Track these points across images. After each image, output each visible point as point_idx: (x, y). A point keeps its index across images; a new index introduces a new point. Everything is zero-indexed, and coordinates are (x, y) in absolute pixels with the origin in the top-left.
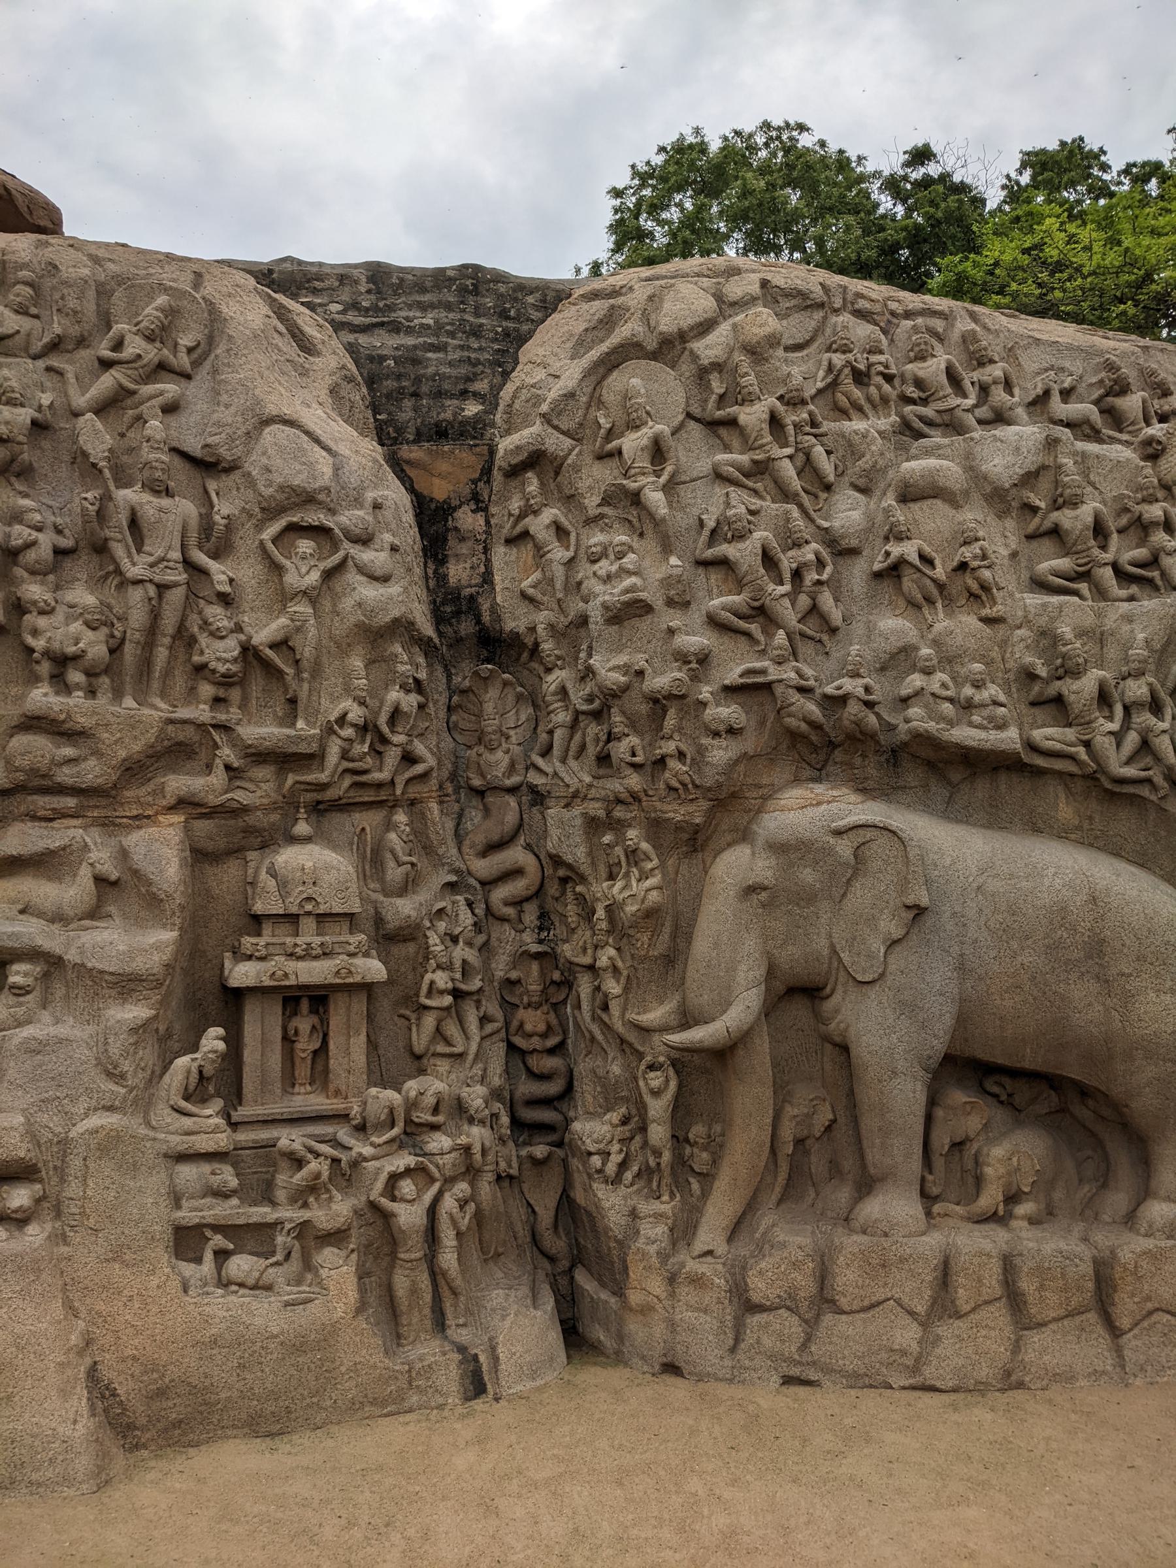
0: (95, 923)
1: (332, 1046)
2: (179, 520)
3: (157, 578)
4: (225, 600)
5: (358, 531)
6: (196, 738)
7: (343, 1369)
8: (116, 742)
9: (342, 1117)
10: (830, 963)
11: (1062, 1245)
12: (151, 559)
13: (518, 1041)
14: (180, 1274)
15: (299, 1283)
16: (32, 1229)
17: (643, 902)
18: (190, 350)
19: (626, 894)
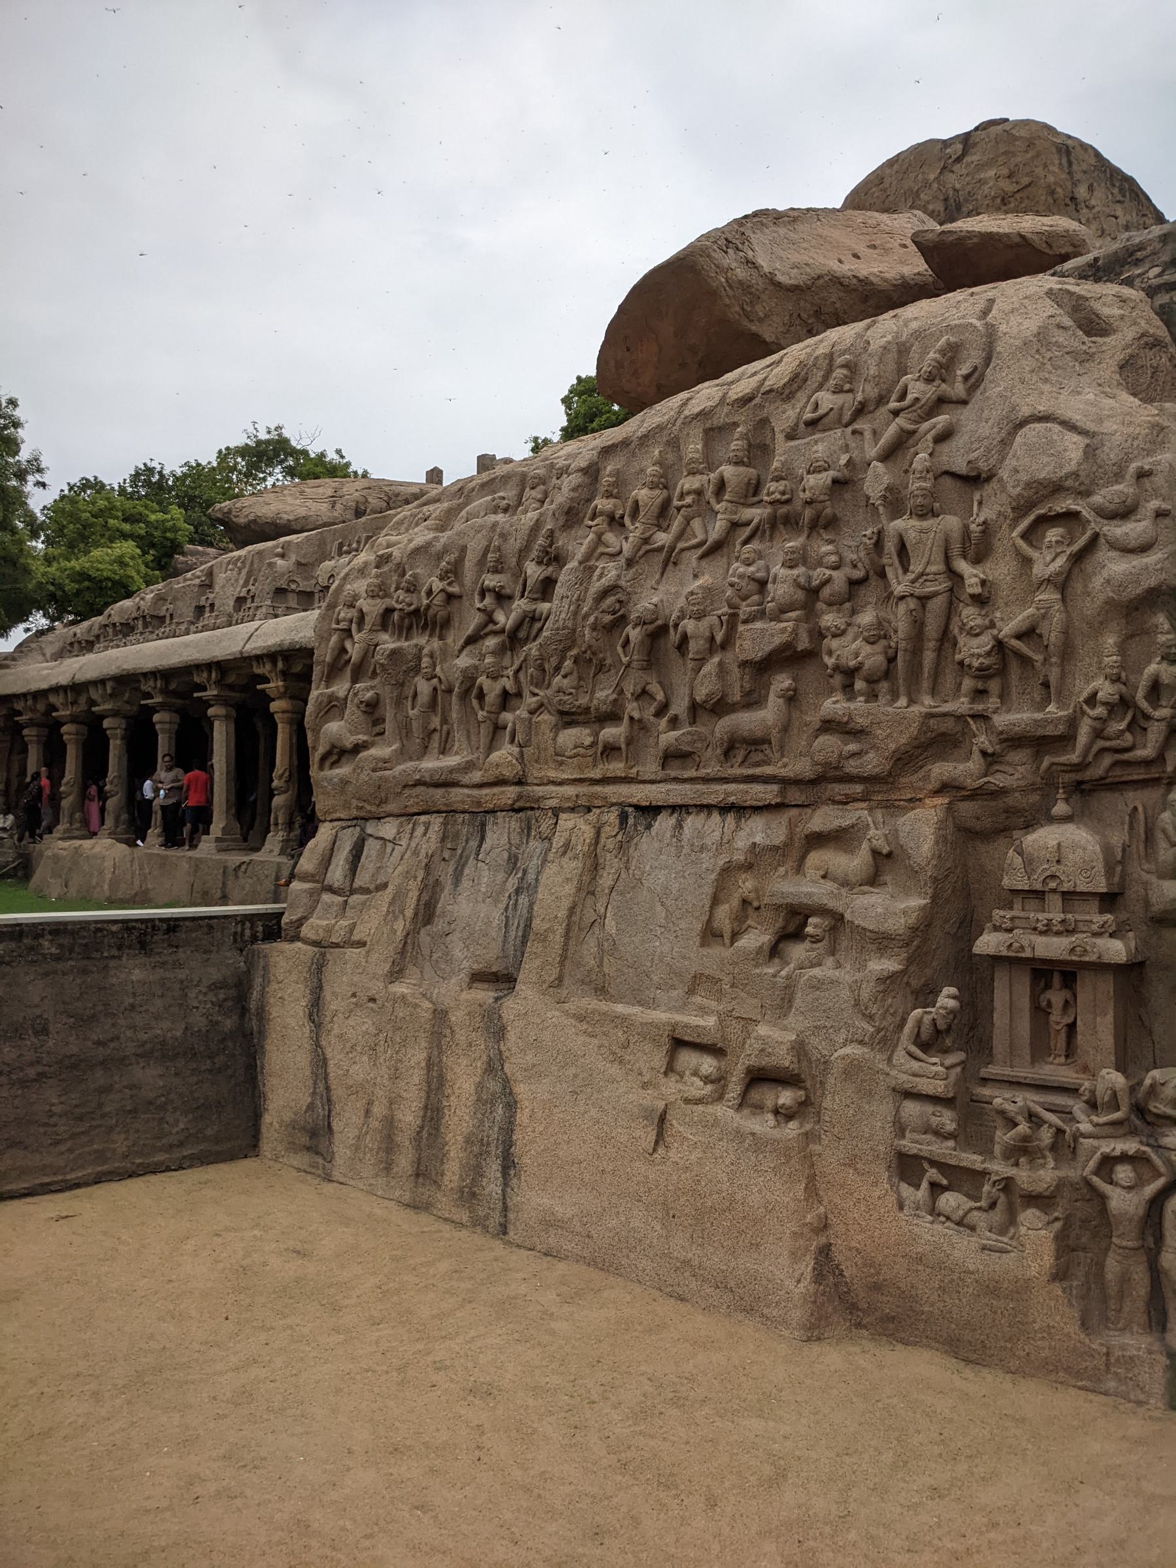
0: (872, 889)
1: (1079, 1023)
2: (940, 536)
3: (918, 592)
4: (980, 601)
5: (1112, 507)
6: (959, 728)
7: (1037, 1326)
8: (887, 736)
9: (1073, 1091)
12: (911, 576)
14: (899, 1193)
15: (1002, 1231)
16: (793, 1125)
18: (966, 378)
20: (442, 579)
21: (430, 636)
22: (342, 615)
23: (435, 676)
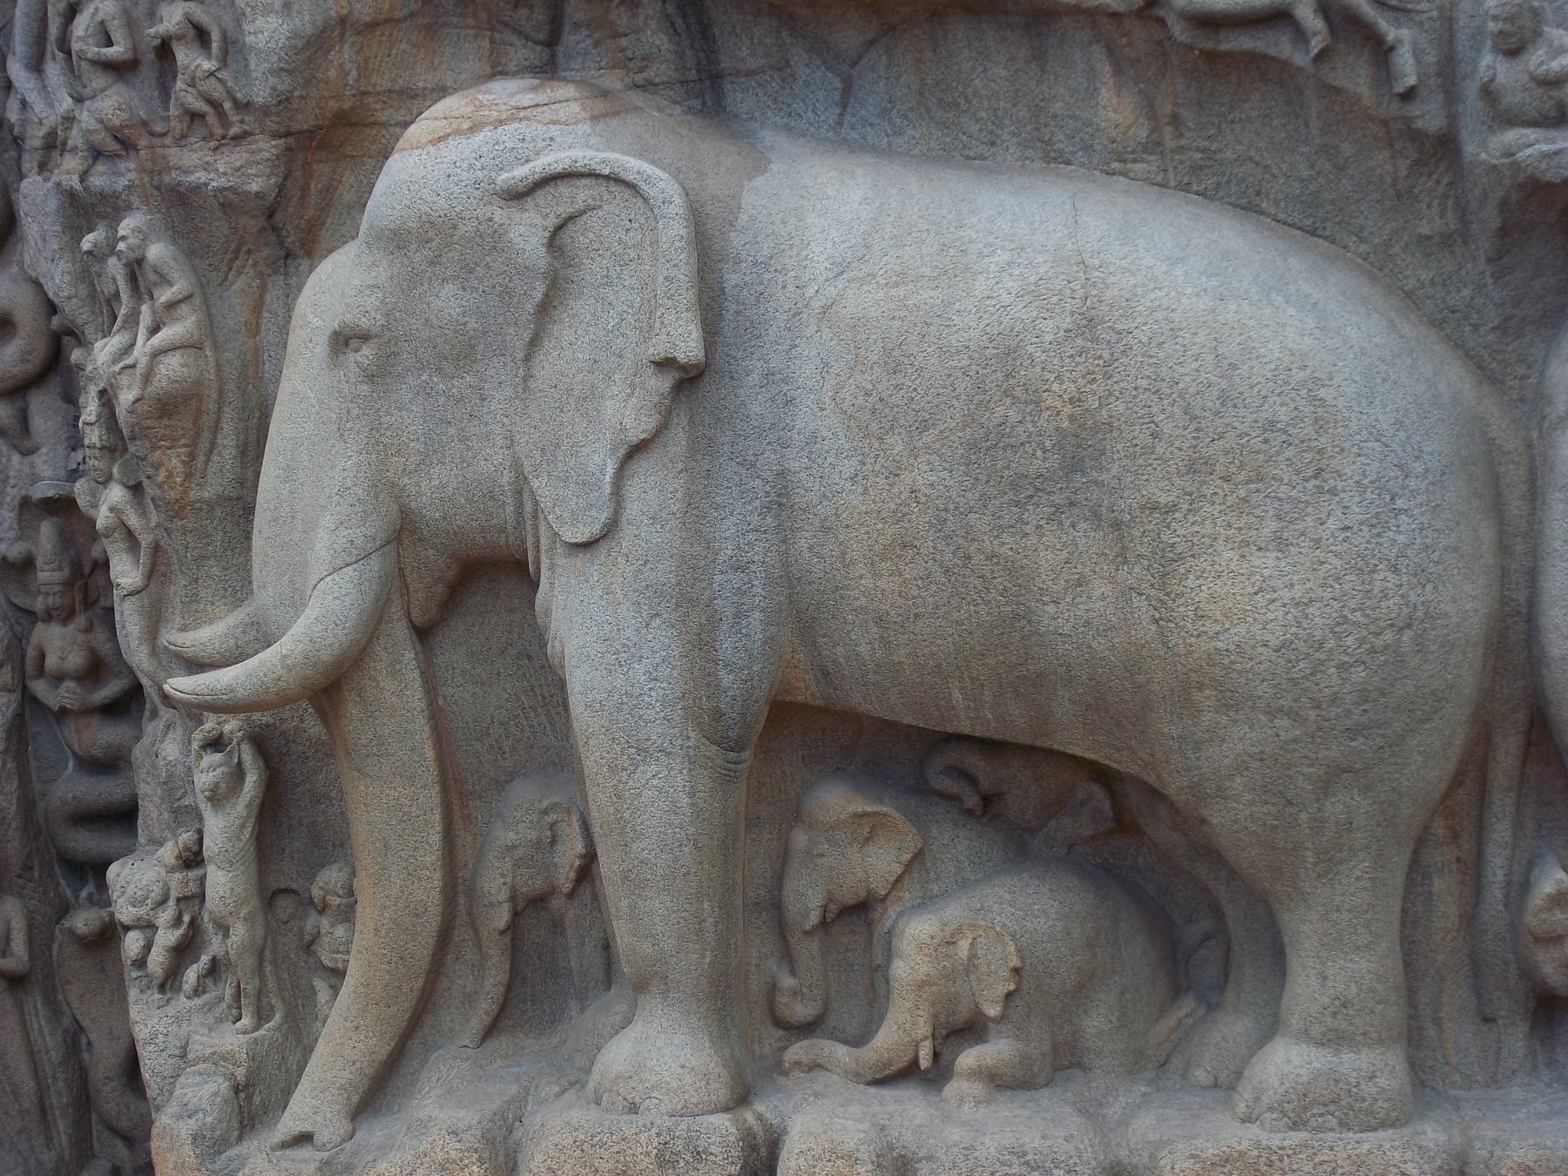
10: (519, 505)
11: (1032, 1140)
13: (39, 688)
17: (147, 379)
19: (117, 368)
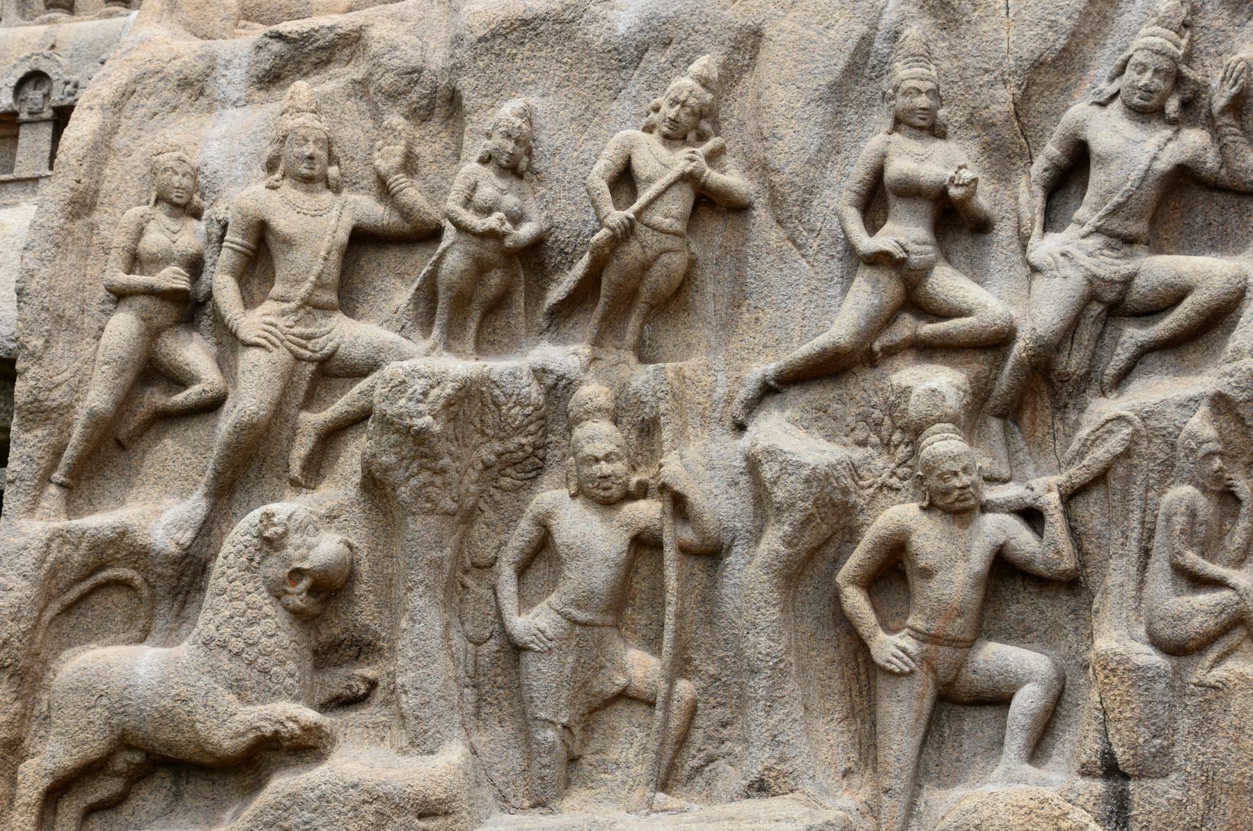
20: (675, 136)
21: (597, 342)
22: (154, 240)
23: (642, 491)
